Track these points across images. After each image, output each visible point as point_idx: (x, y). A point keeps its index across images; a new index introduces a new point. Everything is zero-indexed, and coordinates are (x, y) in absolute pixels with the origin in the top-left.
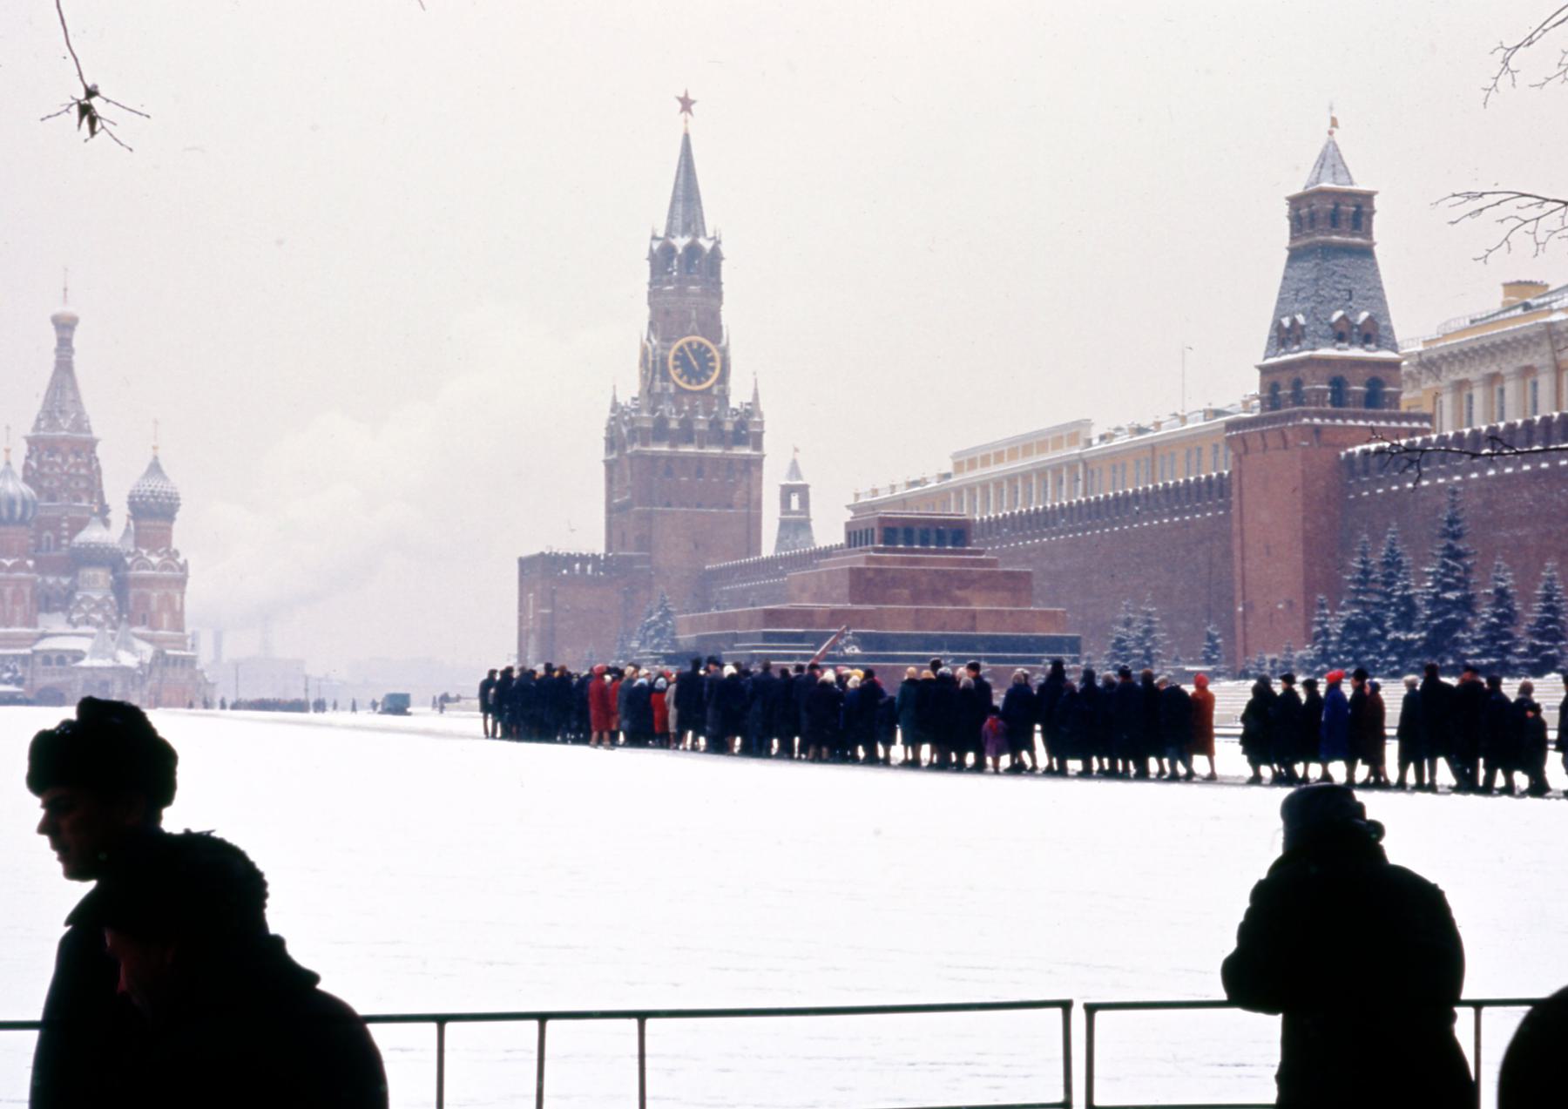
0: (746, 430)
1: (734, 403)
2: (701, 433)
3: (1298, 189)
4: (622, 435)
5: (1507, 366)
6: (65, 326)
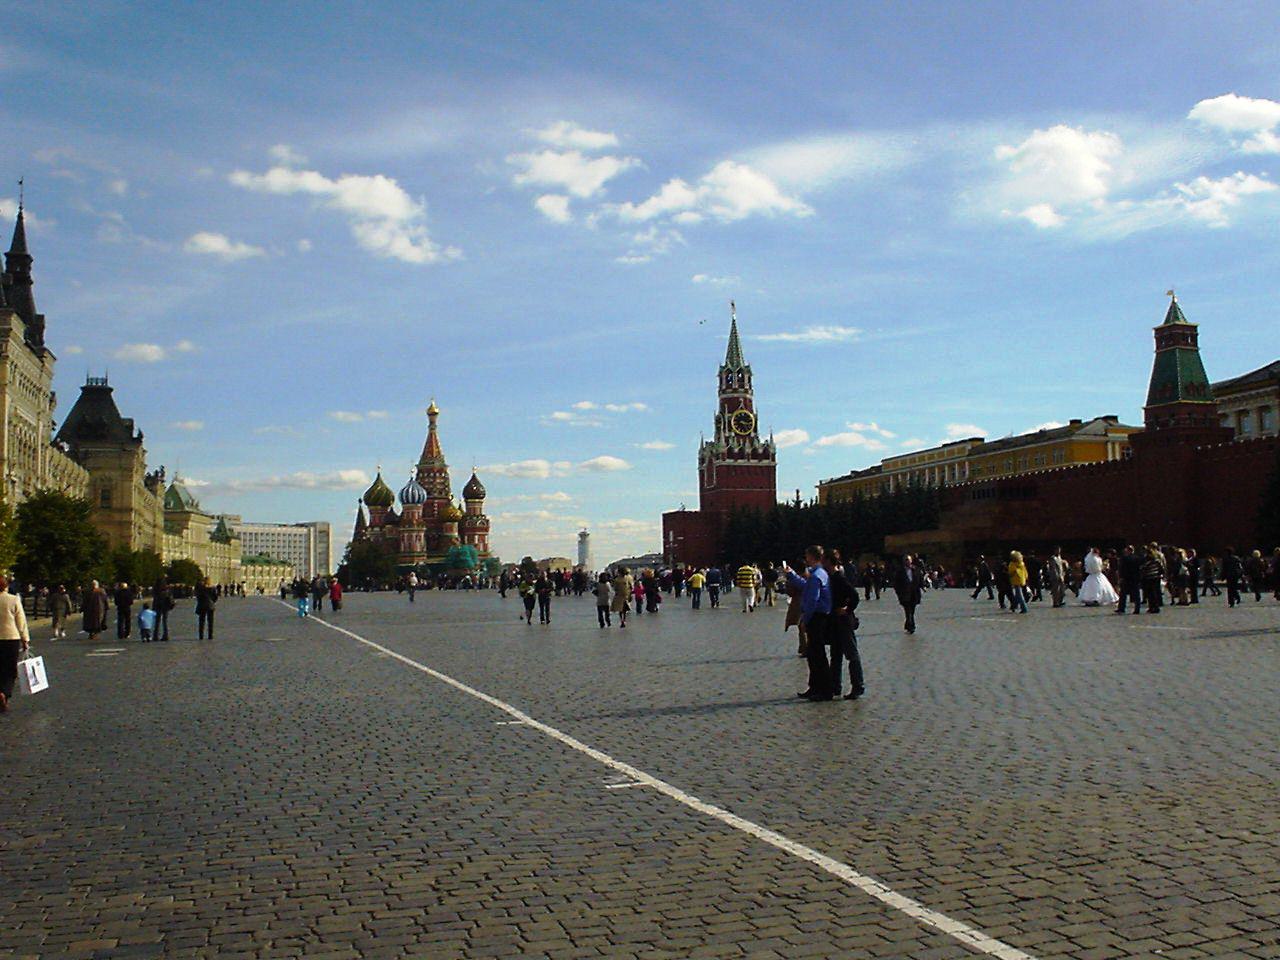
0: (768, 453)
1: (762, 441)
2: (748, 454)
3: (1161, 323)
4: (708, 458)
5: (1252, 405)
6: (432, 414)
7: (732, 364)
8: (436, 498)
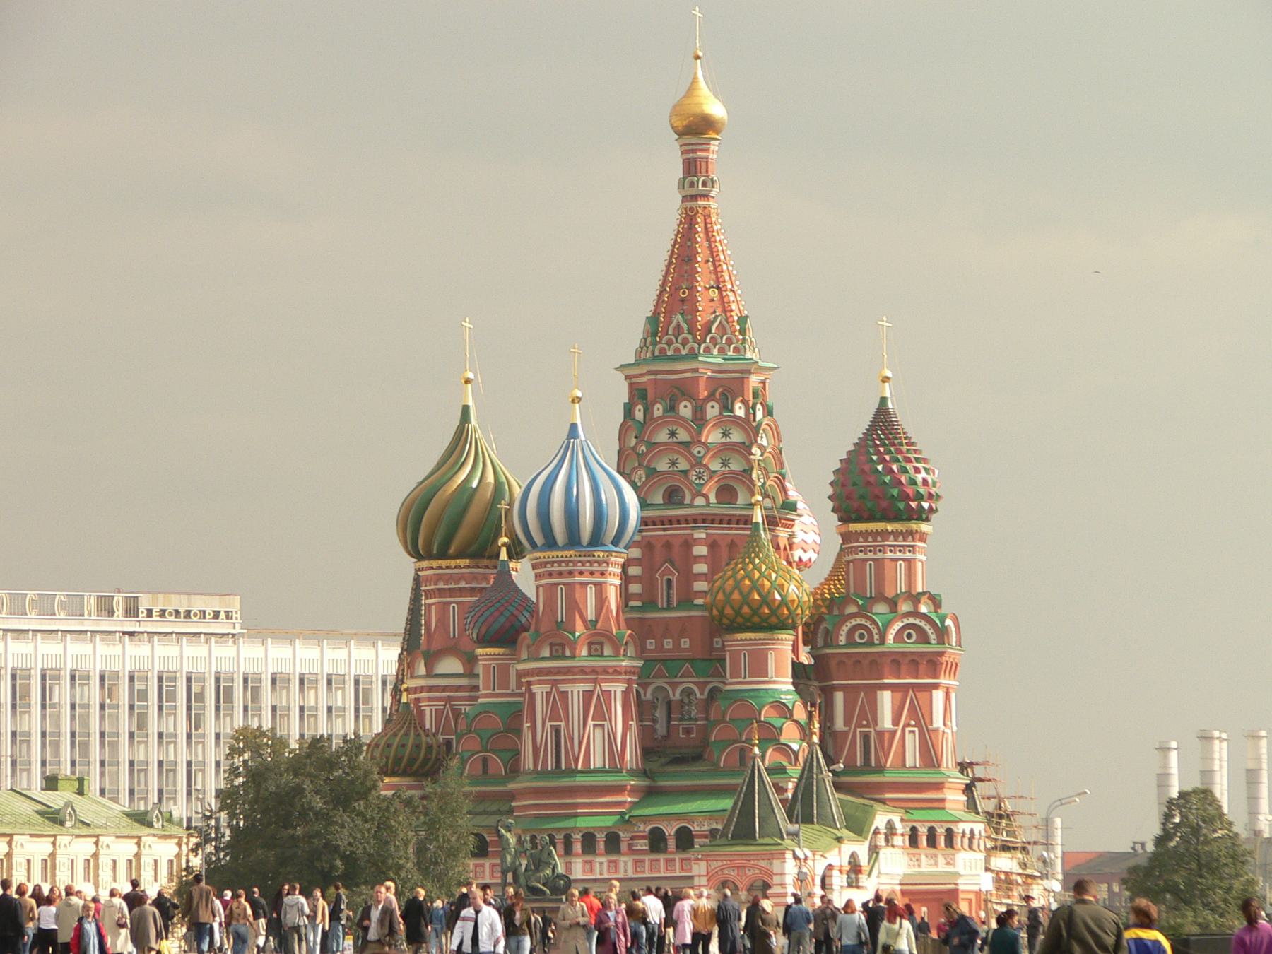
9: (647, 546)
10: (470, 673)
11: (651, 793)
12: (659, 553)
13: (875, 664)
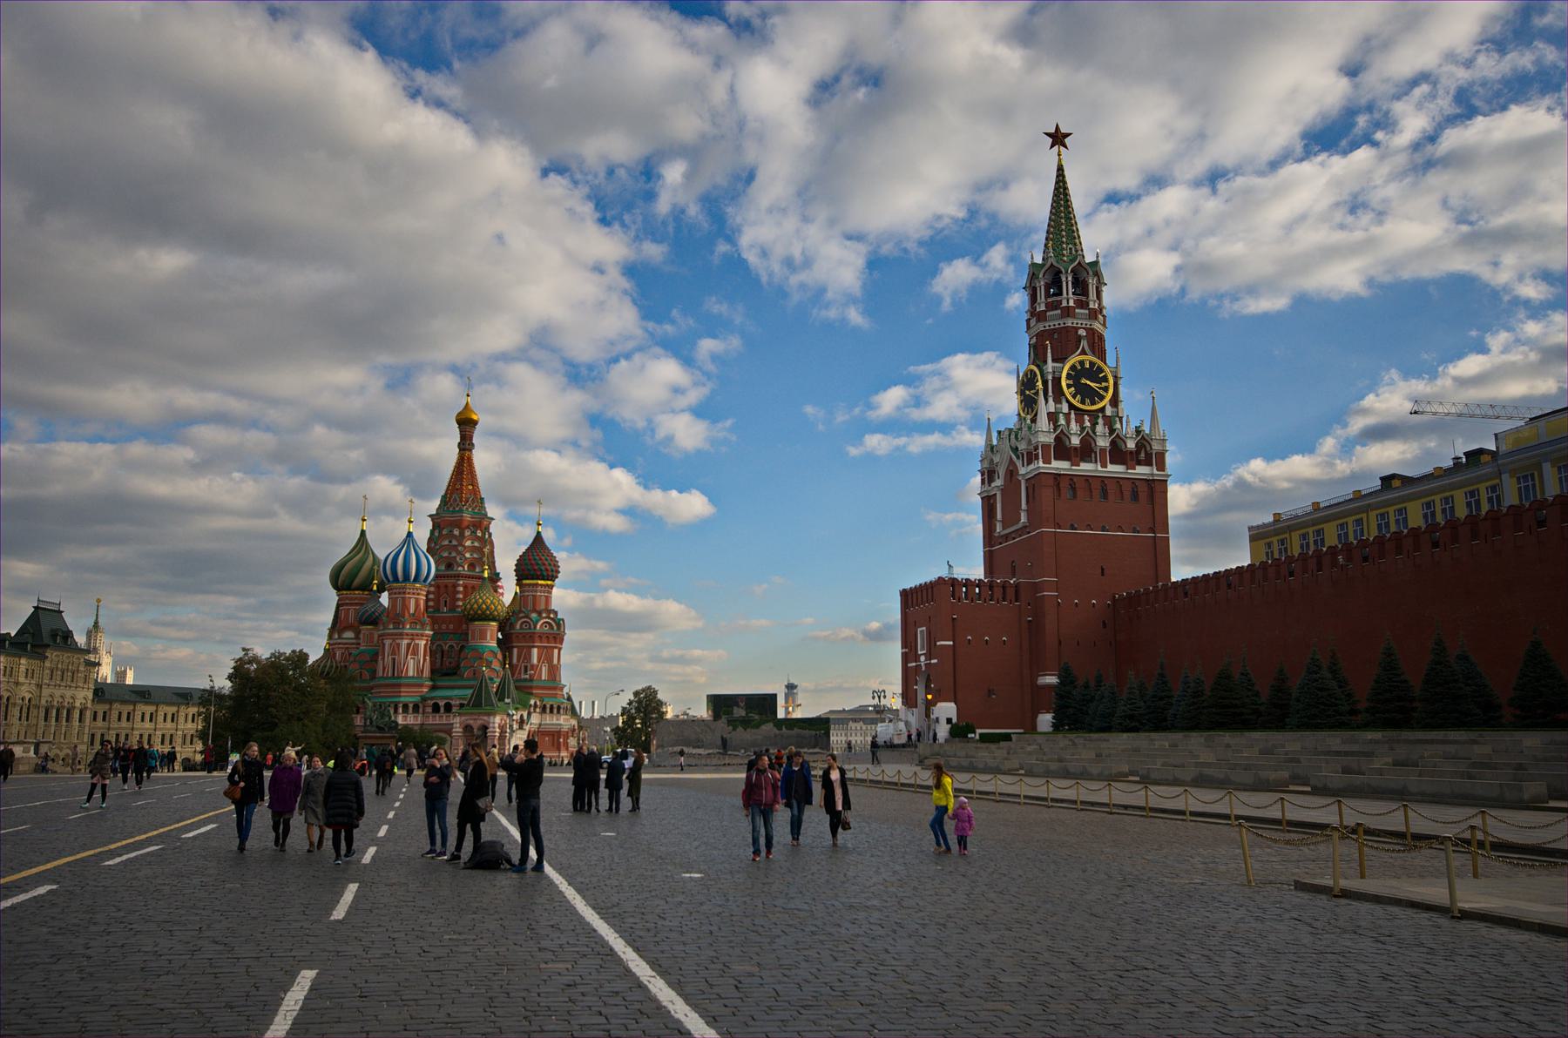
7: (1059, 255)
8: (458, 576)
9: (438, 587)
10: (357, 637)
11: (434, 688)
12: (443, 588)
13: (531, 637)
